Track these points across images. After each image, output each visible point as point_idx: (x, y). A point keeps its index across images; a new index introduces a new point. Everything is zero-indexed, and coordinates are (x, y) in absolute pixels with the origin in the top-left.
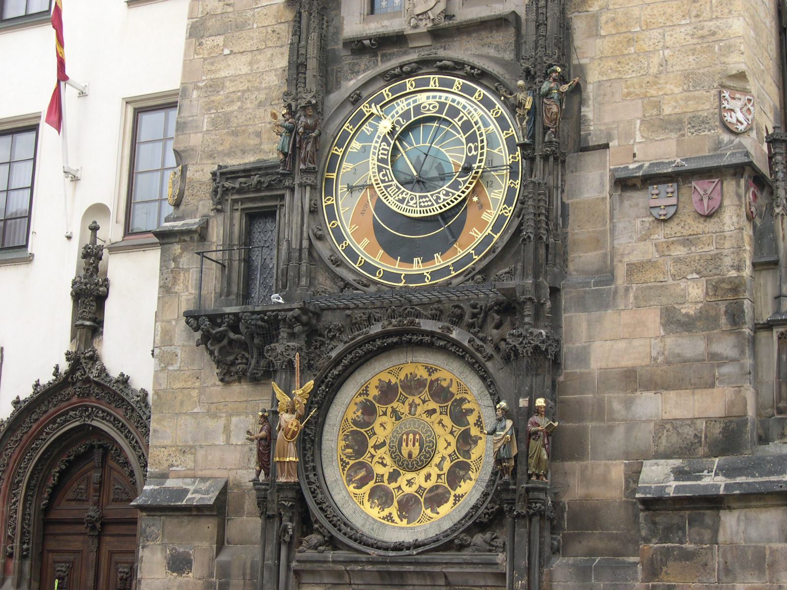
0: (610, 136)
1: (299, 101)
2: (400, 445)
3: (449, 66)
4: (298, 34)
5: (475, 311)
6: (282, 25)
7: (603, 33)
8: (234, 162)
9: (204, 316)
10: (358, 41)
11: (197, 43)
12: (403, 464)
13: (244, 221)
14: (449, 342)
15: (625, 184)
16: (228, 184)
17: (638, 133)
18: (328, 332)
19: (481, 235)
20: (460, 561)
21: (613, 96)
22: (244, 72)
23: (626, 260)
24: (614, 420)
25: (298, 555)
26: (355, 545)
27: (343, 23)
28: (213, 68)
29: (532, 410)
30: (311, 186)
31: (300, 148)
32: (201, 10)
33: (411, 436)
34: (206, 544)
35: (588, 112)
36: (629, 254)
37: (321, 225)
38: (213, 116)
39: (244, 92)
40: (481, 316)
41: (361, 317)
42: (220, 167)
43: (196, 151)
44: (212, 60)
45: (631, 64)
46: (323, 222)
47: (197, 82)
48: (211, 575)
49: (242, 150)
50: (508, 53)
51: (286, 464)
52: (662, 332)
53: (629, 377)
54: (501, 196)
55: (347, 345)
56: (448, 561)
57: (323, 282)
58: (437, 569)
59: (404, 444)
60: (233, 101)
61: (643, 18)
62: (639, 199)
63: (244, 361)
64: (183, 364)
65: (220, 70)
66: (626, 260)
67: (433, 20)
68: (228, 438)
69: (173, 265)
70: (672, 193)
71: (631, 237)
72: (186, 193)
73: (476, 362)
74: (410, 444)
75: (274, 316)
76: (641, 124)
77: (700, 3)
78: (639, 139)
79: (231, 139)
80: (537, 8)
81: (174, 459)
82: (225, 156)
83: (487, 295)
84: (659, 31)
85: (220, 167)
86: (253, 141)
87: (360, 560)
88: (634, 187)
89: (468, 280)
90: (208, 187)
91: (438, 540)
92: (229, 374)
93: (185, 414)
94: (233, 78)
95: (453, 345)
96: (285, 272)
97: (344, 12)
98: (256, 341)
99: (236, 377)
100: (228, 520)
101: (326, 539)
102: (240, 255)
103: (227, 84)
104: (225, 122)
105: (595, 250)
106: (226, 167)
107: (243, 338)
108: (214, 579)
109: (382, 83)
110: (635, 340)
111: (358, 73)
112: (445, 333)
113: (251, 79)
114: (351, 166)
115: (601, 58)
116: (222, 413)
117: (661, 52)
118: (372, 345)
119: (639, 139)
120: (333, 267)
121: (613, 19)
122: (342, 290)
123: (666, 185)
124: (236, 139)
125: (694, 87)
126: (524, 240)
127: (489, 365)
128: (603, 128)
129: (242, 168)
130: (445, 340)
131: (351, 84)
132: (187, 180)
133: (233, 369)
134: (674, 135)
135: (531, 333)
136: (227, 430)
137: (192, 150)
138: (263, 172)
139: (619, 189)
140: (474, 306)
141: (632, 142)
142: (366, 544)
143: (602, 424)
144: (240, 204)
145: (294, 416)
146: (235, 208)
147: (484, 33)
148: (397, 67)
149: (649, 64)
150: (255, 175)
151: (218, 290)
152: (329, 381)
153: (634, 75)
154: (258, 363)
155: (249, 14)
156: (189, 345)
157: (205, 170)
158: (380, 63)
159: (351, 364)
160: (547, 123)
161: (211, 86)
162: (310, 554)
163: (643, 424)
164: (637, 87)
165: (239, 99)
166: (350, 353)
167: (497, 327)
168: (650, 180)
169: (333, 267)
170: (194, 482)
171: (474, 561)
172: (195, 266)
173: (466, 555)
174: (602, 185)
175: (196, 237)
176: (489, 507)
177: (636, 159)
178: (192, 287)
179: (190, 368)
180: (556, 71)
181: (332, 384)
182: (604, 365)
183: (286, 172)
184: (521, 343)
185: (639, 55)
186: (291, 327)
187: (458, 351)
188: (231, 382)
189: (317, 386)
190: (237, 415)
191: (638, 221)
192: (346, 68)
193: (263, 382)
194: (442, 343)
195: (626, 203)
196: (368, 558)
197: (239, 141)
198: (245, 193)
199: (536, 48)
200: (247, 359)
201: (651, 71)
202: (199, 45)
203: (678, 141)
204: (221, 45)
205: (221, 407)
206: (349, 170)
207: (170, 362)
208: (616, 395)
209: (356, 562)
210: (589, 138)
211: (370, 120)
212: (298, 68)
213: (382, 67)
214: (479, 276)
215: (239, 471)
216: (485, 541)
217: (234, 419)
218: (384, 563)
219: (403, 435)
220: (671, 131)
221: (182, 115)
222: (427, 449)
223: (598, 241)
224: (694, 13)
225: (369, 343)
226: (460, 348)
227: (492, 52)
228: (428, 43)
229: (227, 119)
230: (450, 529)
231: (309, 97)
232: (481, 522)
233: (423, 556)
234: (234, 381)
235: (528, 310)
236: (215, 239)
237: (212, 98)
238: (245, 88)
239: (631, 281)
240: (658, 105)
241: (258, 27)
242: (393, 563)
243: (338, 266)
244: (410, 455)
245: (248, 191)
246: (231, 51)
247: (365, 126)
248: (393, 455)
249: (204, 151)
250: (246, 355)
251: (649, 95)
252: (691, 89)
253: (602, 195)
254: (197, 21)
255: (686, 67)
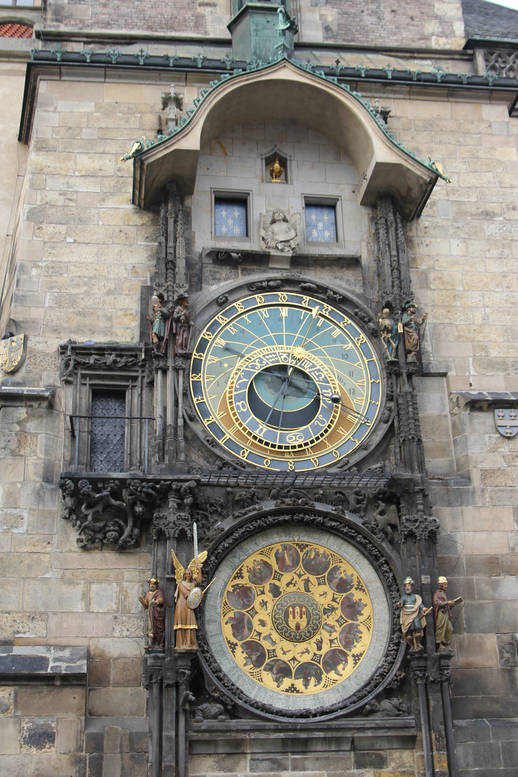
0: (448, 367)
1: (170, 293)
2: (286, 616)
3: (313, 288)
4: (165, 235)
5: (360, 497)
6: (131, 227)
7: (432, 287)
8: (82, 340)
9: (85, 478)
10: (225, 253)
11: (36, 227)
12: (290, 636)
13: (91, 396)
14: (341, 523)
15: (475, 405)
16: (79, 359)
17: (471, 367)
18: (210, 507)
19: (347, 434)
20: (373, 726)
21: (447, 336)
22: (90, 260)
23: (480, 466)
24: (483, 598)
25: (195, 724)
26: (258, 712)
27: (194, 236)
28: (54, 252)
29: (434, 587)
30: (184, 370)
31: (175, 335)
32: (39, 198)
33: (297, 609)
34: (71, 716)
35: (428, 346)
36: (481, 462)
37: (190, 407)
38: (56, 294)
39: (90, 278)
40: (365, 502)
41: (245, 495)
42: (70, 342)
43: (38, 324)
44: (54, 245)
45: (459, 314)
46: (192, 405)
47: (37, 261)
48: (79, 749)
49: (91, 330)
50: (358, 287)
51: (189, 632)
52: (516, 526)
53: (492, 563)
54: (364, 403)
55: (239, 520)
56: (361, 726)
57: (198, 460)
58: (349, 734)
59: (291, 616)
60: (78, 285)
61: (464, 281)
62: (484, 420)
63: (116, 528)
64: (31, 527)
65: (63, 254)
66: (480, 466)
67: (293, 249)
68: (88, 604)
69: (18, 428)
70: (515, 416)
71: (481, 448)
72: (27, 361)
73: (370, 543)
74: (298, 616)
75: (167, 485)
76: (473, 361)
77: (509, 278)
78: (473, 372)
79: (78, 318)
80: (391, 256)
81: (21, 625)
82: (71, 332)
83: (370, 483)
84: (480, 293)
85: (70, 342)
86: (103, 324)
87: (267, 728)
88: (481, 409)
89: (346, 471)
90: (53, 359)
91: (345, 707)
92: (93, 540)
93: (35, 578)
94: (78, 264)
95: (345, 526)
96: (161, 446)
97: (195, 227)
98: (139, 509)
99: (99, 545)
100: (90, 690)
101: (229, 708)
102: (88, 428)
103: (72, 268)
104: (70, 302)
105: (443, 456)
106: (75, 343)
107: (124, 504)
108: (83, 754)
109: (247, 292)
110: (494, 533)
111: (219, 280)
112: (340, 514)
113: (98, 268)
114: (217, 359)
115: (433, 306)
116: (80, 580)
117: (483, 309)
118: (262, 521)
119: (473, 372)
120: (210, 447)
121: (440, 278)
122: (220, 468)
123: (509, 410)
124: (83, 319)
125: (513, 339)
126: (404, 440)
127: (384, 545)
128: (442, 360)
129: (97, 346)
130: (336, 521)
131: (214, 289)
132: (28, 349)
133: (100, 536)
134: (502, 374)
135: (426, 519)
136: (86, 597)
137: (33, 322)
138: (118, 353)
139: (468, 409)
140: (357, 493)
141: (467, 374)
142: (272, 713)
143: (473, 602)
144: (88, 379)
145: (193, 584)
146: (84, 382)
147: (335, 268)
148: (264, 281)
149: (473, 317)
150: (111, 354)
151: (68, 458)
152: (220, 553)
153: (462, 322)
154: (132, 531)
155: (94, 212)
156: (39, 510)
157: (49, 343)
158: (240, 276)
159: (241, 537)
160: (408, 346)
161: (53, 268)
162: (206, 724)
163: (509, 603)
164: (467, 332)
165: (85, 284)
166: (241, 527)
167: (382, 513)
168: (498, 404)
169: (210, 447)
170: (48, 650)
171: (387, 726)
172: (44, 432)
173: (377, 720)
174: (443, 404)
175: (45, 404)
176: (398, 674)
177: (472, 388)
178: (41, 452)
179: (40, 532)
180: (413, 306)
181: (221, 556)
182: (469, 552)
183: (160, 354)
184: (416, 528)
185: (465, 309)
186: (181, 497)
187: (350, 532)
188: (90, 549)
189: (209, 557)
190: (97, 583)
191: (487, 436)
192: (207, 274)
193: (128, 550)
194: (333, 524)
195: (476, 421)
196: (277, 726)
197: (88, 322)
198: (95, 370)
199: (393, 287)
200: (120, 526)
201: (476, 322)
202: (39, 229)
203: (505, 378)
204: (64, 232)
205: (78, 574)
206: (214, 362)
207: (15, 525)
208: (483, 578)
209: (261, 730)
210: (431, 366)
211: (234, 322)
212: (167, 263)
213: (243, 279)
214: (355, 468)
215: (102, 640)
216: (394, 706)
217: (95, 587)
218: (294, 730)
219: (289, 607)
220: (499, 370)
221: (21, 288)
222: (314, 621)
223: (444, 450)
224: (505, 285)
225: (260, 519)
226: (352, 529)
227: (344, 284)
228: (289, 267)
229: (73, 301)
230: (354, 695)
231: (181, 291)
232: (391, 689)
233: (335, 723)
234: (96, 548)
235: (419, 499)
236: (62, 408)
237: (54, 278)
238: (92, 275)
239: (485, 484)
240: (484, 348)
241: (103, 224)
242: (302, 730)
243: (213, 446)
244: (298, 627)
245: (99, 369)
246: (75, 241)
247: (229, 326)
248: (280, 627)
249: (47, 326)
250: (121, 522)
251: (477, 339)
252: (511, 340)
253: (443, 413)
254: (35, 208)
255: (504, 323)
